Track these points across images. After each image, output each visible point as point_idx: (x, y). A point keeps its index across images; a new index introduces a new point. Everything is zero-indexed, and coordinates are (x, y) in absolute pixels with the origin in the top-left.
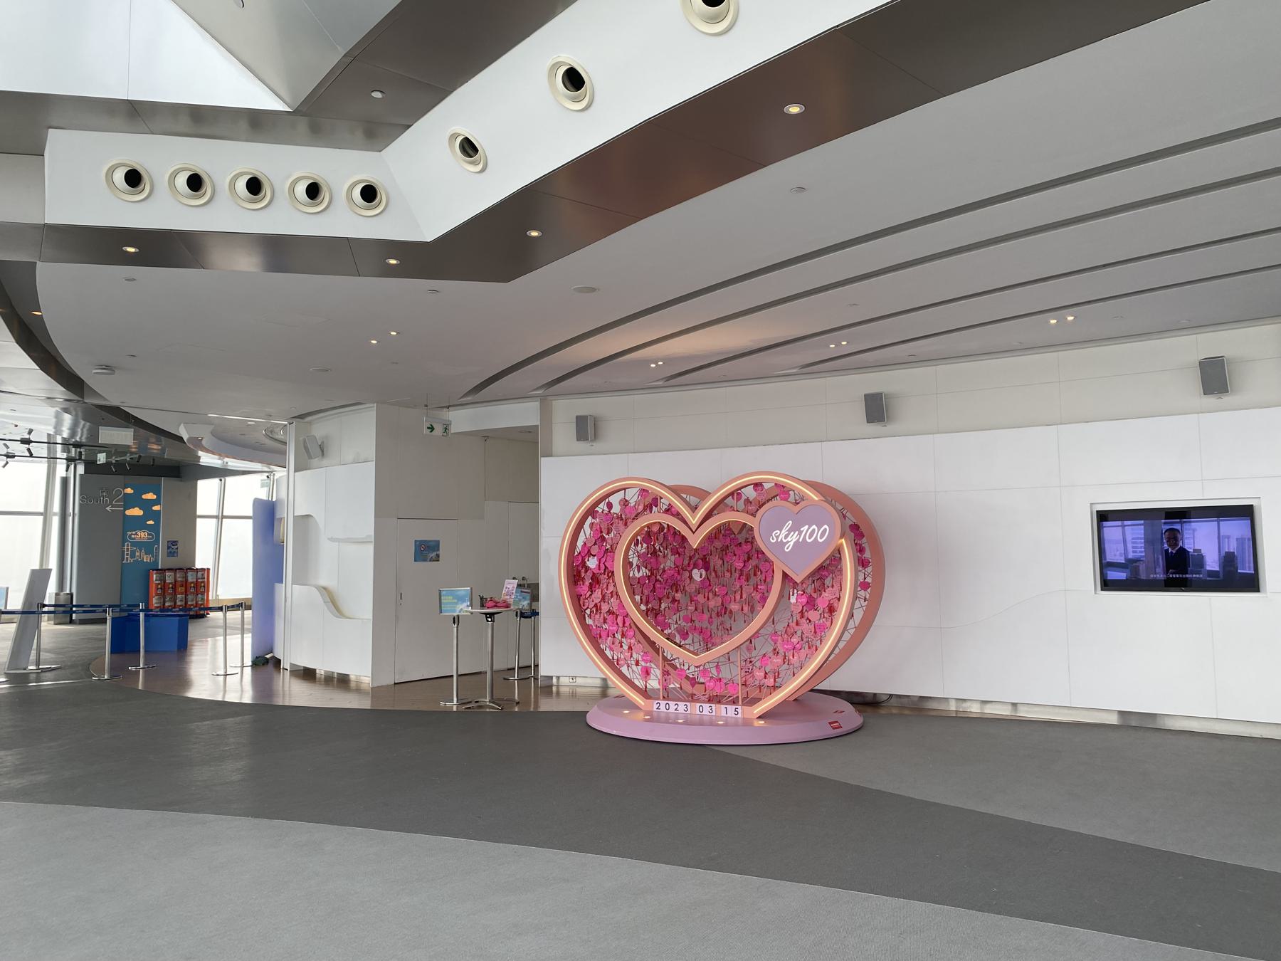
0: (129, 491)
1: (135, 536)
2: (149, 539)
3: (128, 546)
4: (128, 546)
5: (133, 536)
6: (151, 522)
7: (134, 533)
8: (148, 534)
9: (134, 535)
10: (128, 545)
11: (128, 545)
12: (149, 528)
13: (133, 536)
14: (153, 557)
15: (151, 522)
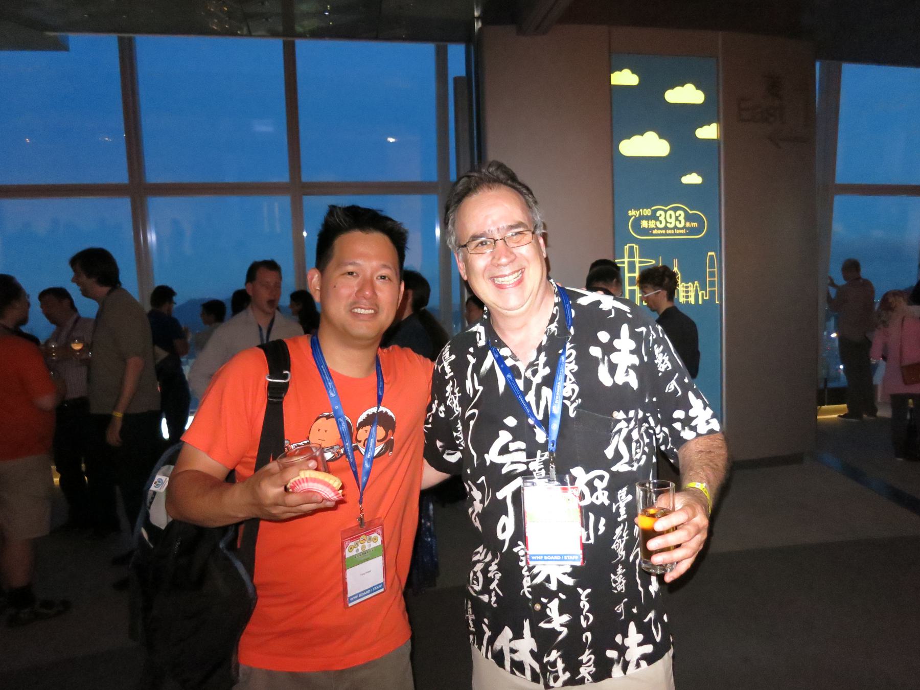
0: (625, 78)
1: (652, 224)
2: (691, 231)
3: (631, 255)
4: (631, 255)
5: (644, 224)
6: (693, 179)
7: (647, 212)
8: (688, 218)
9: (647, 218)
10: (631, 248)
11: (631, 248)
12: (690, 195)
13: (644, 224)
14: (703, 287)
15: (693, 179)
